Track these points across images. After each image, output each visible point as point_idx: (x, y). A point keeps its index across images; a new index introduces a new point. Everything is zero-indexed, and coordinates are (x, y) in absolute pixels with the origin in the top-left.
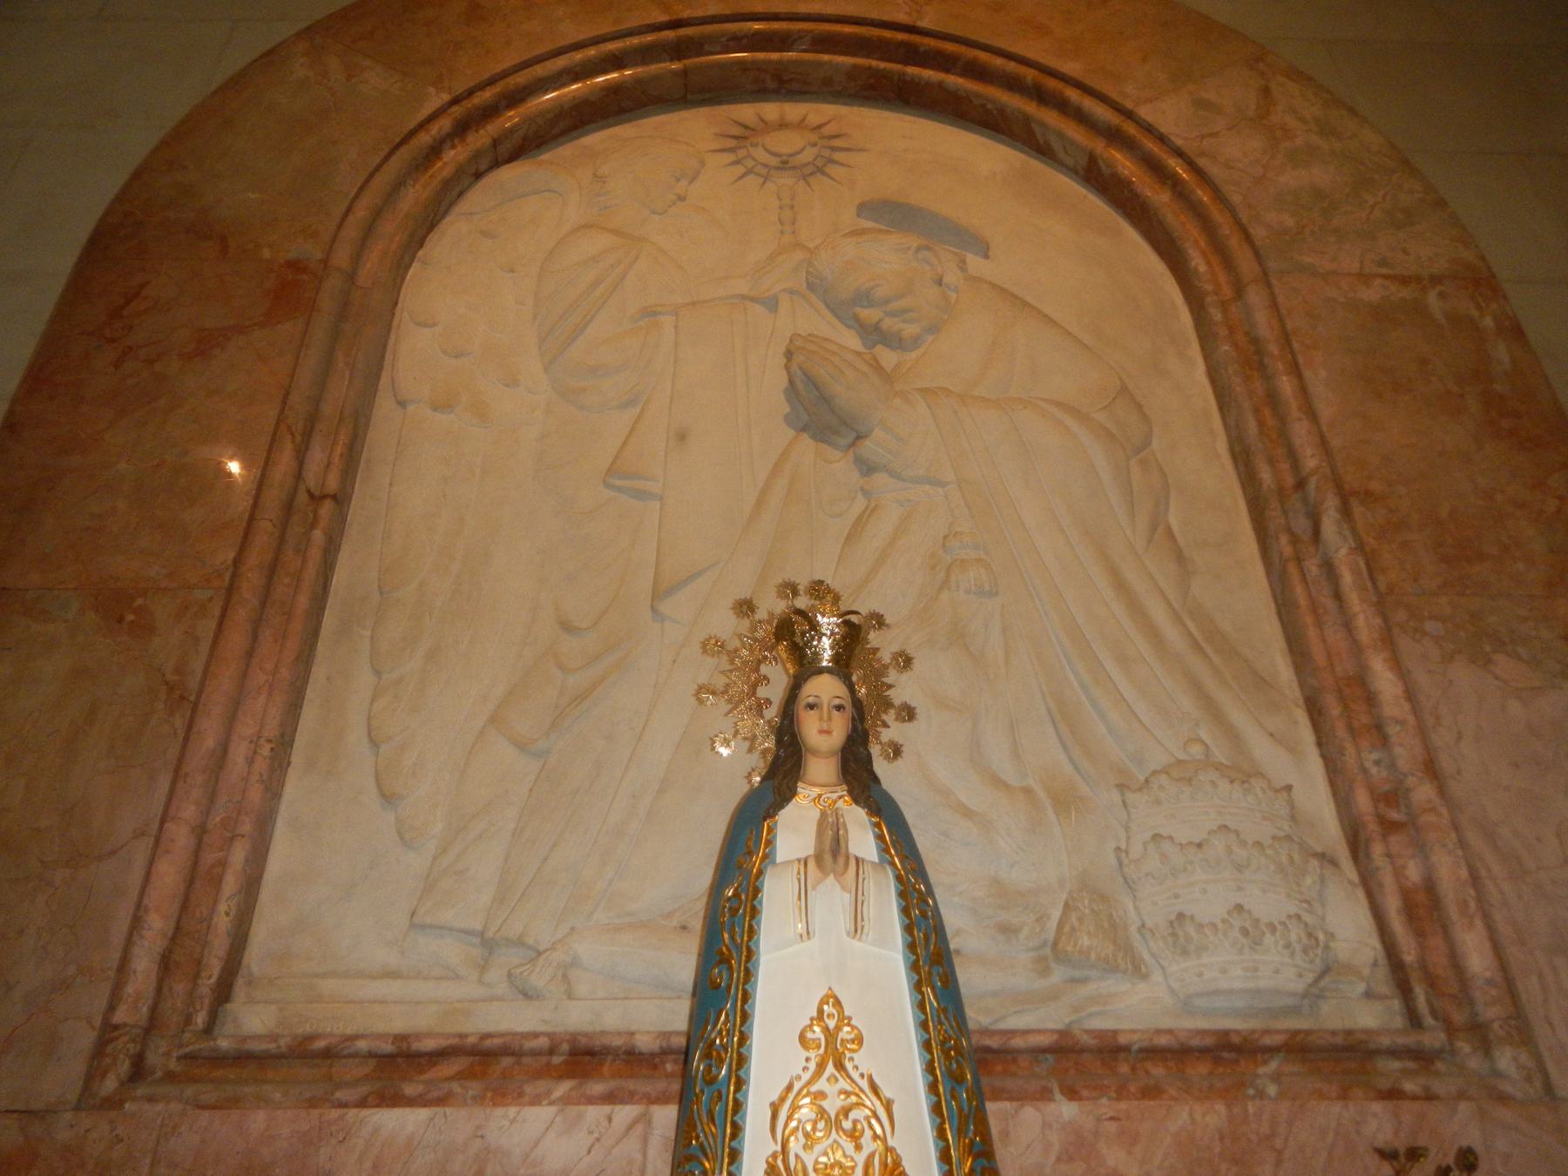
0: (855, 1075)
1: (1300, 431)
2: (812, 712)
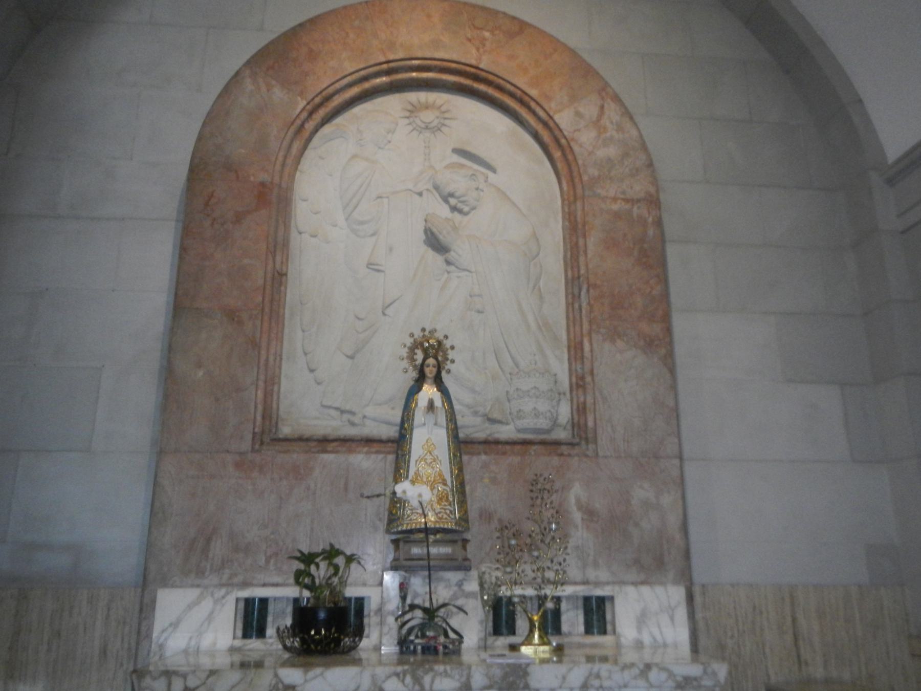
0: (434, 455)
1: (582, 259)
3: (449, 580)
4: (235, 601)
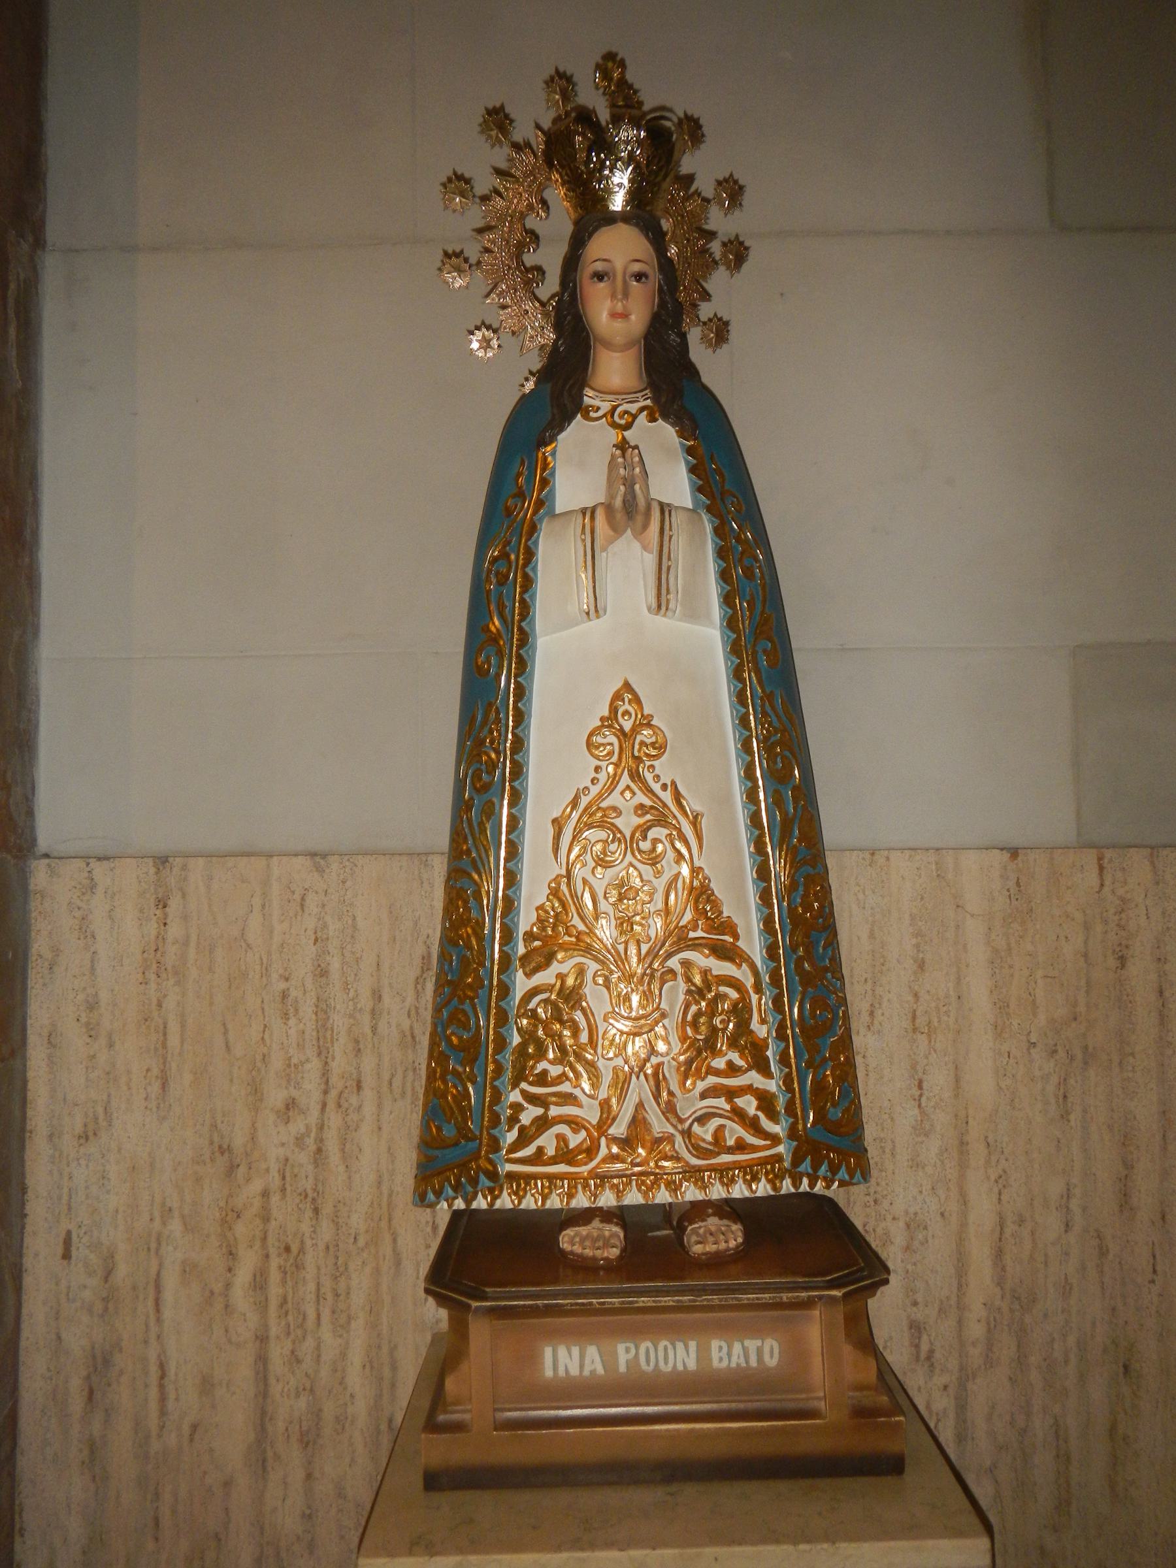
0: (656, 787)
2: (602, 285)
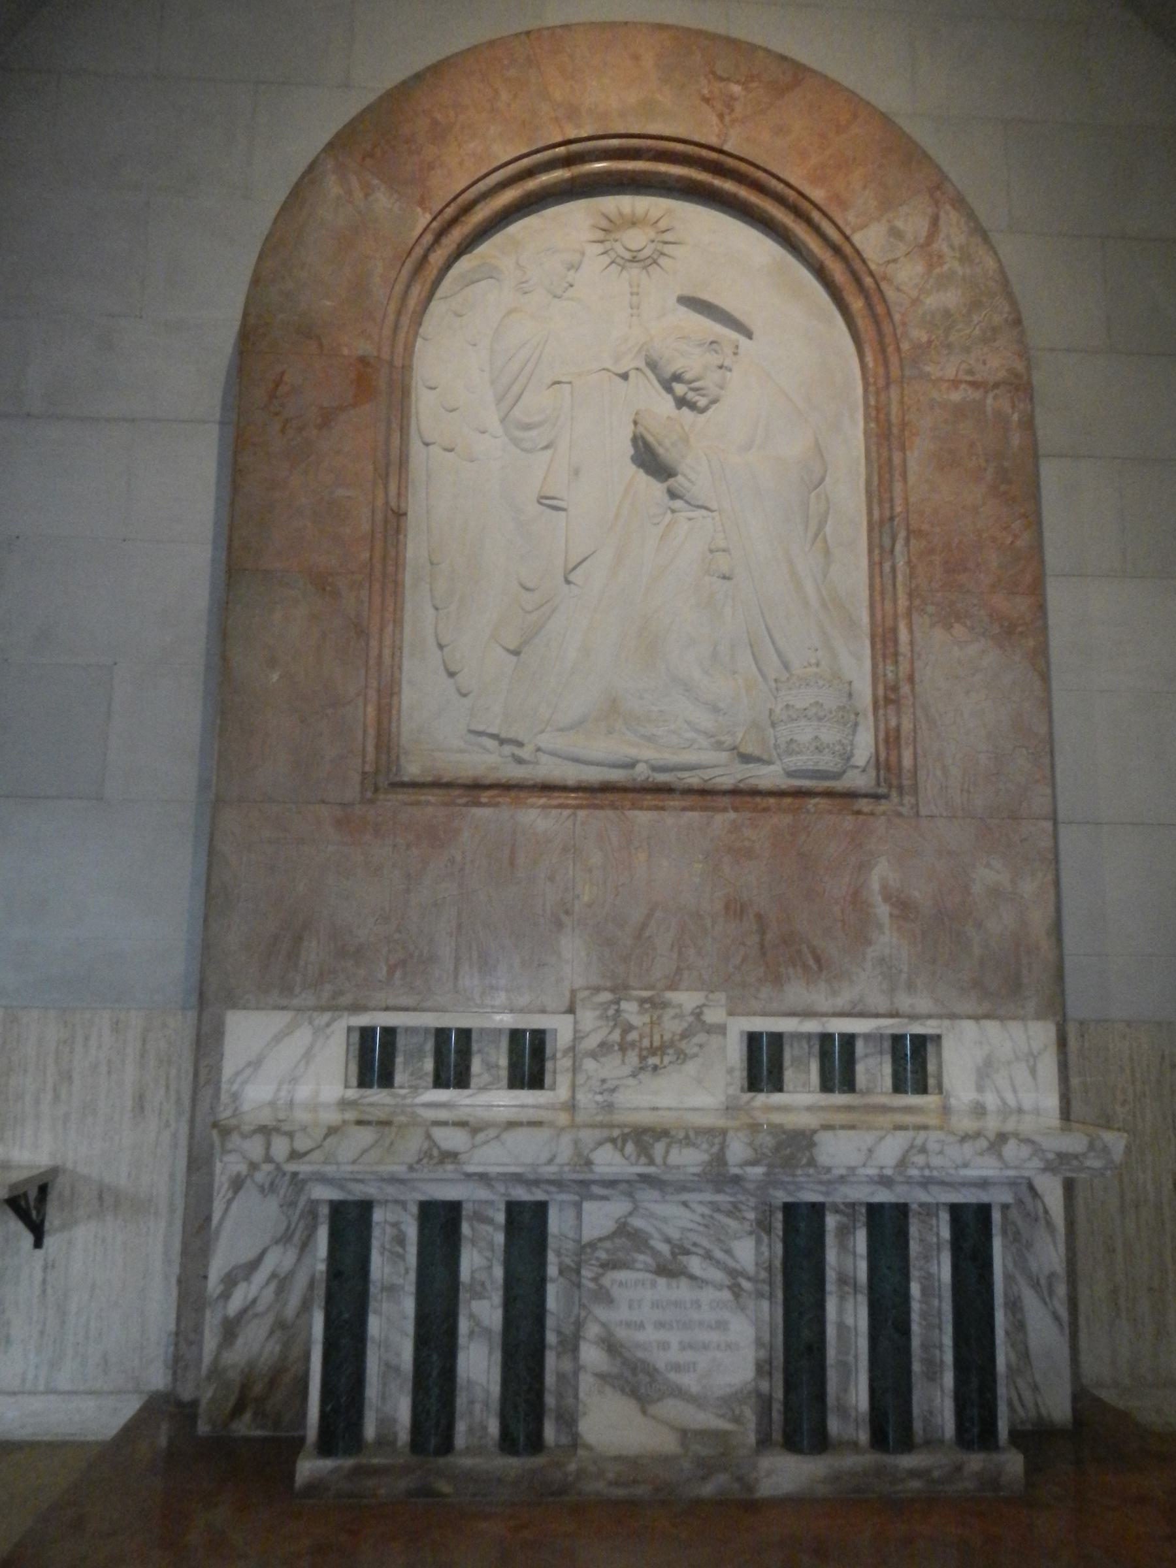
1: (898, 487)
3: (680, 1006)
4: (346, 1031)
